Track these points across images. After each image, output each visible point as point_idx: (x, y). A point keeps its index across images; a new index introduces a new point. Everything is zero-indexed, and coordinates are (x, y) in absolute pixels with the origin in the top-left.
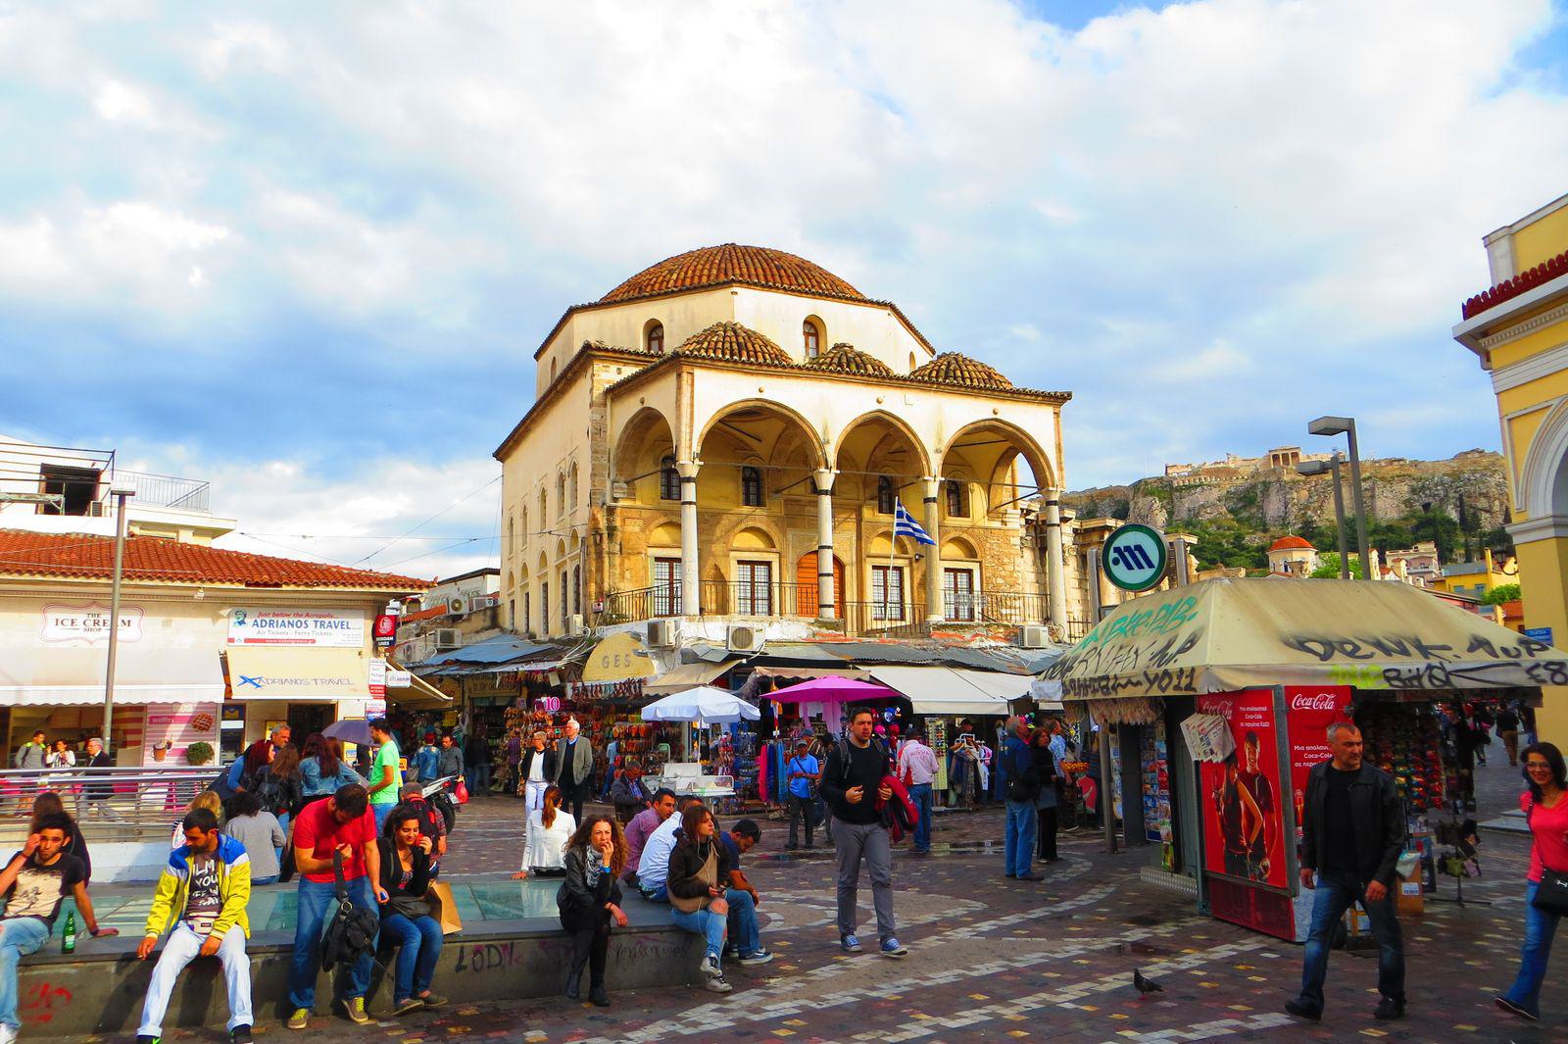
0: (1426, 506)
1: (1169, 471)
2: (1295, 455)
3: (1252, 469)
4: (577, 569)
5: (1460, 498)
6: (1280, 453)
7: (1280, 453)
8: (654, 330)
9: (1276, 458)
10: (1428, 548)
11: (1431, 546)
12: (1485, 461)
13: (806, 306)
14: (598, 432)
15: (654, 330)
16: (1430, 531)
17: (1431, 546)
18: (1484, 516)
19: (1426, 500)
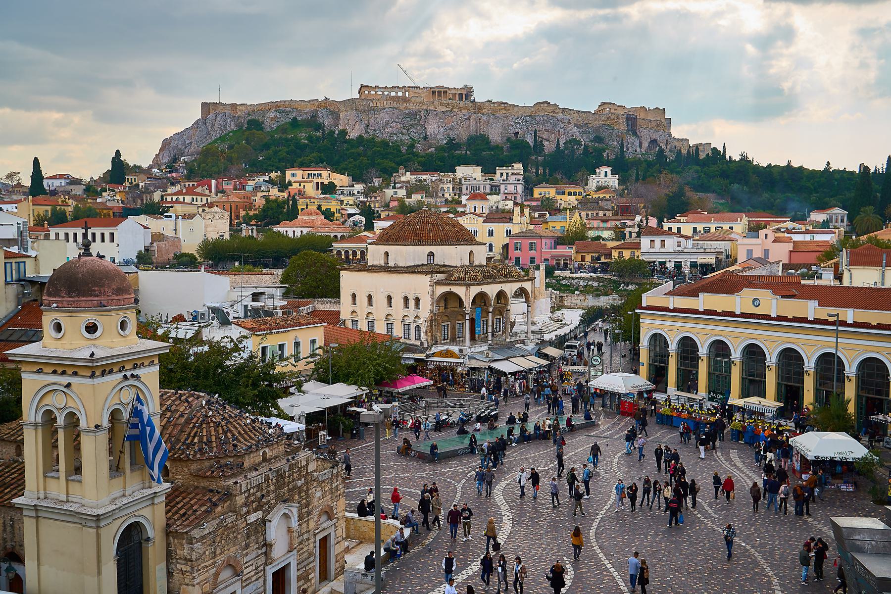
0: (517, 134)
1: (363, 89)
2: (445, 92)
3: (420, 100)
4: (418, 328)
5: (535, 133)
6: (437, 90)
7: (437, 90)
8: (431, 255)
9: (434, 92)
10: (518, 167)
11: (520, 166)
12: (550, 109)
13: (469, 248)
14: (432, 295)
15: (431, 255)
16: (517, 152)
17: (520, 166)
18: (546, 143)
19: (517, 130)
